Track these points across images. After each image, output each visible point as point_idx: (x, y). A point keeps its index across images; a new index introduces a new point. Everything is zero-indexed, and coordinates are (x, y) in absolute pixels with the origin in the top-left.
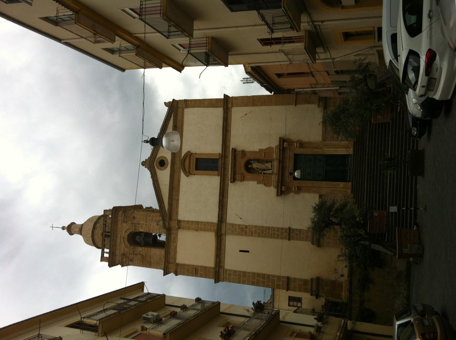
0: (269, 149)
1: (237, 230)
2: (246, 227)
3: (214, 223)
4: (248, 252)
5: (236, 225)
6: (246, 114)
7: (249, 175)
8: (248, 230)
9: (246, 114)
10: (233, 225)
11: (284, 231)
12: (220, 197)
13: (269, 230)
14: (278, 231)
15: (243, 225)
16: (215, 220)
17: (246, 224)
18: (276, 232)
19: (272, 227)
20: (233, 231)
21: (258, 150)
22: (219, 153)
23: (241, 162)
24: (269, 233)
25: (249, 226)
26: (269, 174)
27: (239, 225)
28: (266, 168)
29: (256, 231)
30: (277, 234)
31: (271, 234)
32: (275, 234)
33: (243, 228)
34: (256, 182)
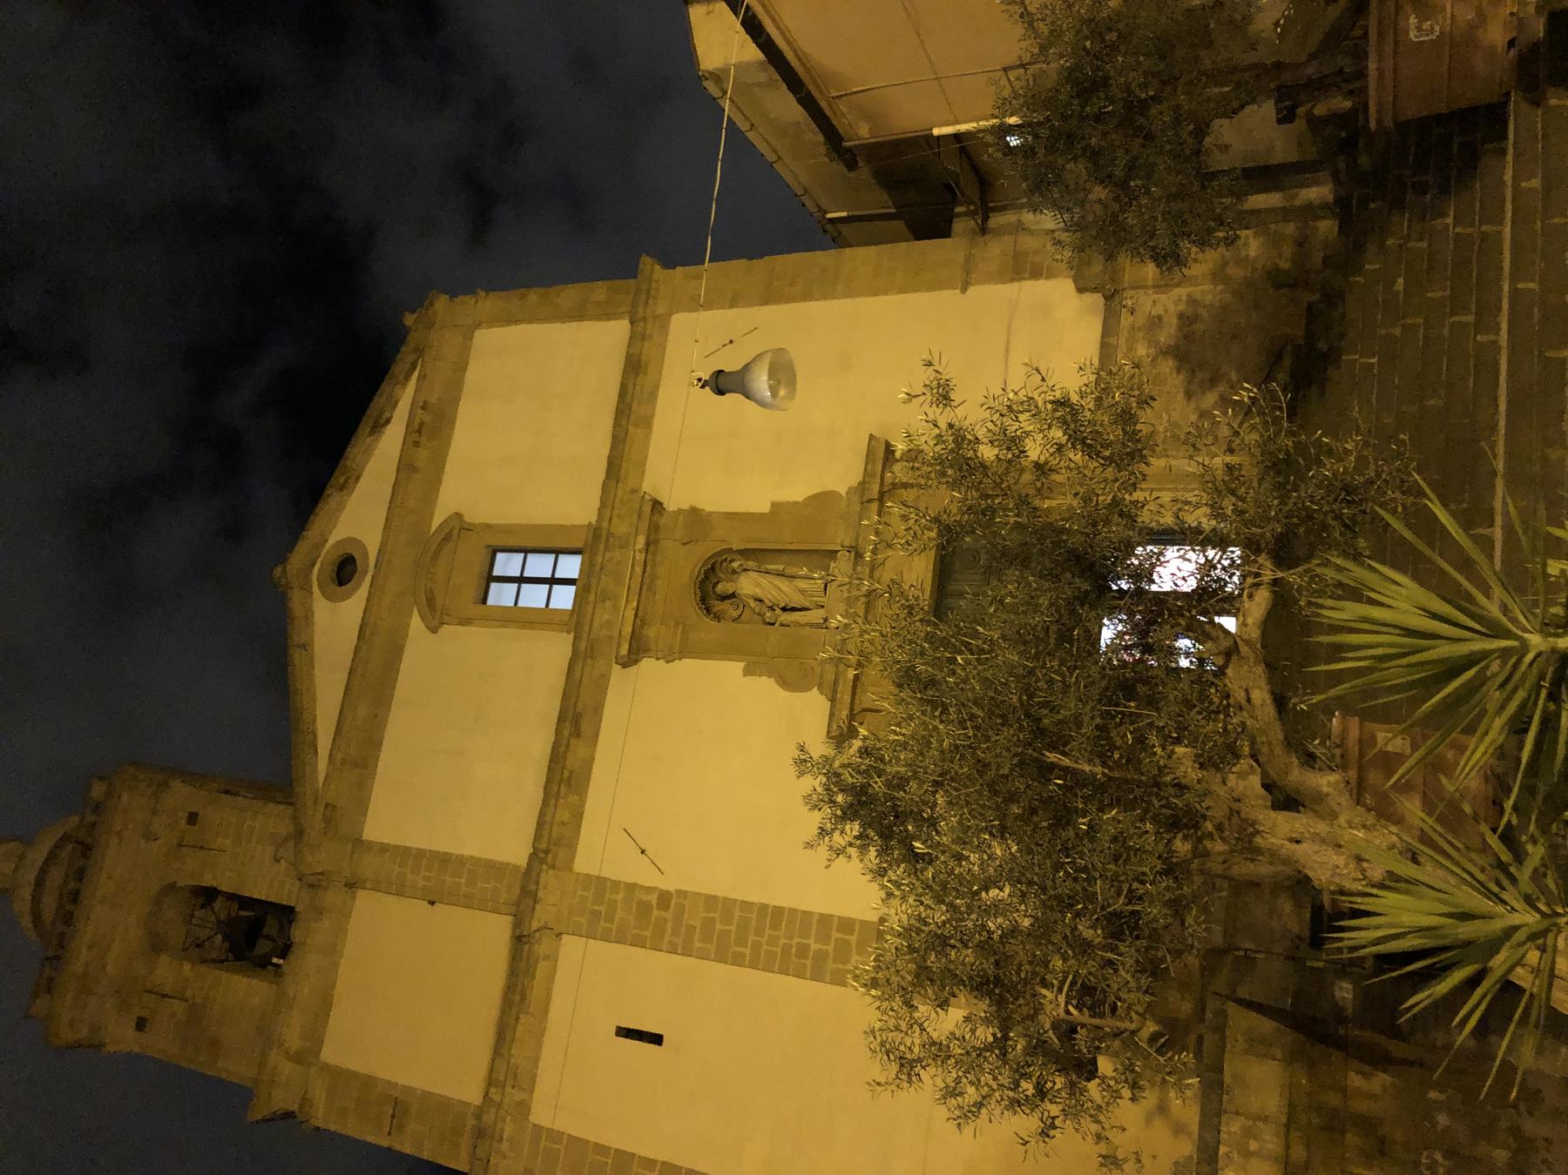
0: (822, 500)
1: (619, 914)
2: (665, 898)
3: (516, 867)
4: (657, 1039)
5: (616, 885)
6: (731, 342)
7: (709, 630)
8: (669, 915)
9: (731, 342)
10: (600, 885)
11: (853, 939)
12: (558, 731)
13: (775, 926)
14: (824, 937)
15: (649, 890)
16: (516, 852)
17: (664, 887)
18: (811, 942)
19: (793, 911)
20: (596, 914)
21: (765, 508)
22: (590, 523)
23: (681, 566)
24: (773, 941)
25: (681, 894)
26: (811, 625)
27: (632, 887)
28: (797, 600)
29: (709, 924)
30: (818, 952)
31: (786, 949)
32: (803, 951)
33: (648, 905)
34: (742, 665)
